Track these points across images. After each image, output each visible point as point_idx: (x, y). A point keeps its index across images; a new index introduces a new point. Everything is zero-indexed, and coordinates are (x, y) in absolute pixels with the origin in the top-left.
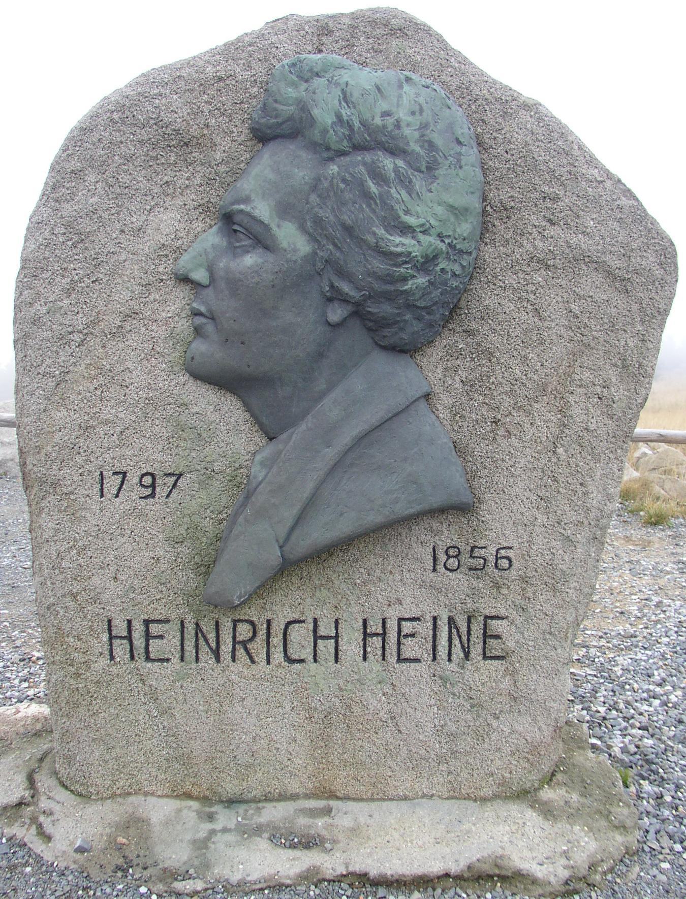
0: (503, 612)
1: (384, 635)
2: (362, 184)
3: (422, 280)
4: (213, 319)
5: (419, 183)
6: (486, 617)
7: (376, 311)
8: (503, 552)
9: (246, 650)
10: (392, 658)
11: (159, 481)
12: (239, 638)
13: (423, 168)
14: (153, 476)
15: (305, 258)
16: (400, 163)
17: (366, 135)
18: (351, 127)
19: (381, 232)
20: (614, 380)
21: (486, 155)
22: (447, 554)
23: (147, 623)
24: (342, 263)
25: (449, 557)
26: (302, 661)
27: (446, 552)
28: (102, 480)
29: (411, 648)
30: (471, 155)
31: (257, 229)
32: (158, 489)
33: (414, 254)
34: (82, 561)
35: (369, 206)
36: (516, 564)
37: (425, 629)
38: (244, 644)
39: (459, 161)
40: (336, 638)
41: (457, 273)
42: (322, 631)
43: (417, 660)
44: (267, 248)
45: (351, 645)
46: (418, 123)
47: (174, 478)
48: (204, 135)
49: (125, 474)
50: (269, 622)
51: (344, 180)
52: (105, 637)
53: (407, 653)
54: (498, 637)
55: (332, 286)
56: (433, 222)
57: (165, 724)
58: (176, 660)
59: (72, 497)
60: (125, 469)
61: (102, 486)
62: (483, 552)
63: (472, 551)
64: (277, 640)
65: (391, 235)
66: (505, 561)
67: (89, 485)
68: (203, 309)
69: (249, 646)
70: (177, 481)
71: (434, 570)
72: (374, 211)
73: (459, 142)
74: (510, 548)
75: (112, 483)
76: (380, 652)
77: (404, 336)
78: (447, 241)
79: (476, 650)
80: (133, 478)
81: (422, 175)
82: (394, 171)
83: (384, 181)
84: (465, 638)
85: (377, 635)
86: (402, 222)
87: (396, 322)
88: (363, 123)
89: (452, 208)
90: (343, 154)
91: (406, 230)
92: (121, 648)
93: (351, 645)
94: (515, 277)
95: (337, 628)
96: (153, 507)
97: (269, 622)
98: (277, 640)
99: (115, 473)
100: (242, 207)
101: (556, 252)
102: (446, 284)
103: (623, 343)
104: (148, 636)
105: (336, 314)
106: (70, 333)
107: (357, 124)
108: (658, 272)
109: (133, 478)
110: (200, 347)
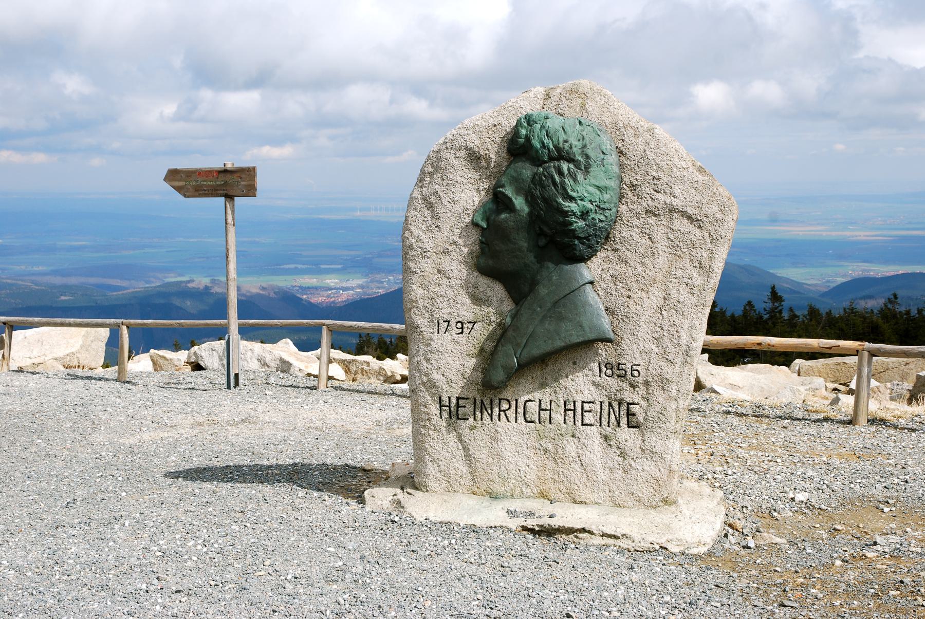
0: (636, 401)
1: (574, 410)
5: (580, 177)
6: (629, 404)
8: (635, 367)
10: (579, 424)
16: (571, 166)
18: (549, 149)
19: (560, 200)
20: (695, 274)
23: (458, 399)
29: (589, 418)
30: (613, 158)
38: (504, 411)
42: (543, 406)
43: (591, 425)
45: (558, 417)
52: (438, 406)
53: (586, 421)
54: (634, 415)
55: (540, 228)
64: (521, 410)
73: (603, 153)
79: (624, 421)
80: (453, 324)
88: (555, 146)
91: (572, 199)
93: (558, 417)
96: (462, 339)
97: (517, 401)
98: (521, 410)
104: (458, 406)
107: (551, 146)
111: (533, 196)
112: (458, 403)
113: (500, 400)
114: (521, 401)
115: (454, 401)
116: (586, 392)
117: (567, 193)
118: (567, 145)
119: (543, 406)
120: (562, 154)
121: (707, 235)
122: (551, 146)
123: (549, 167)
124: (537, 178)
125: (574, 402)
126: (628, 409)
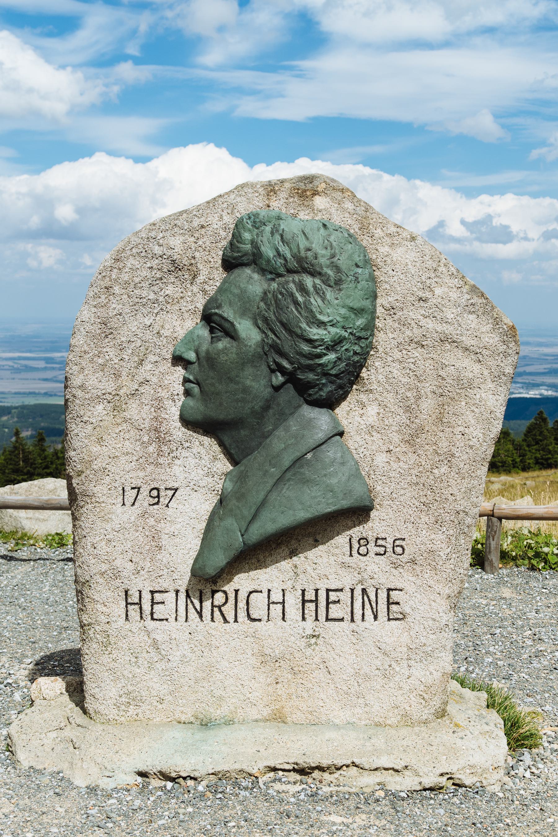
1: (316, 601)
2: (292, 295)
3: (332, 356)
4: (198, 384)
6: (389, 590)
7: (303, 377)
8: (398, 543)
11: (162, 493)
12: (216, 603)
13: (332, 284)
14: (158, 489)
15: (257, 345)
16: (317, 281)
17: (295, 264)
18: (285, 259)
20: (473, 421)
21: (379, 272)
22: (359, 543)
23: (152, 592)
24: (280, 346)
25: (360, 546)
26: (260, 620)
28: (124, 493)
31: (227, 325)
32: (161, 500)
33: (326, 340)
34: (108, 550)
35: (297, 309)
37: (345, 597)
38: (219, 607)
39: (357, 278)
41: (357, 352)
44: (232, 337)
46: (329, 254)
47: (173, 491)
48: (192, 264)
49: (139, 488)
50: (237, 591)
51: (281, 293)
54: (398, 603)
55: (274, 361)
56: (338, 319)
57: (164, 667)
58: (172, 619)
59: (103, 505)
60: (139, 485)
61: (124, 496)
63: (385, 552)
64: (242, 604)
65: (311, 328)
66: (398, 548)
67: (115, 496)
68: (191, 378)
70: (175, 493)
71: (351, 555)
72: (300, 314)
74: (404, 539)
75: (131, 494)
76: (314, 615)
77: (322, 393)
78: (349, 331)
80: (145, 491)
81: (331, 289)
82: (313, 287)
83: (306, 293)
84: (374, 605)
85: (311, 601)
86: (317, 320)
87: (318, 385)
89: (352, 309)
90: (280, 275)
91: (321, 324)
92: (134, 611)
93: (293, 610)
94: (400, 353)
95: (284, 595)
97: (237, 591)
98: (242, 604)
99: (133, 488)
100: (217, 311)
101: (427, 336)
102: (349, 360)
103: (478, 396)
104: (153, 603)
105: (279, 379)
106: (104, 394)
107: (289, 256)
109: (145, 491)
110: (191, 402)
111: (266, 320)
112: (153, 599)
113: (214, 592)
114: (242, 596)
115: (147, 597)
117: (314, 317)
118: (309, 254)
119: (273, 599)
120: (304, 266)
123: (287, 282)
124: (270, 296)
125: (317, 591)
126: (388, 595)
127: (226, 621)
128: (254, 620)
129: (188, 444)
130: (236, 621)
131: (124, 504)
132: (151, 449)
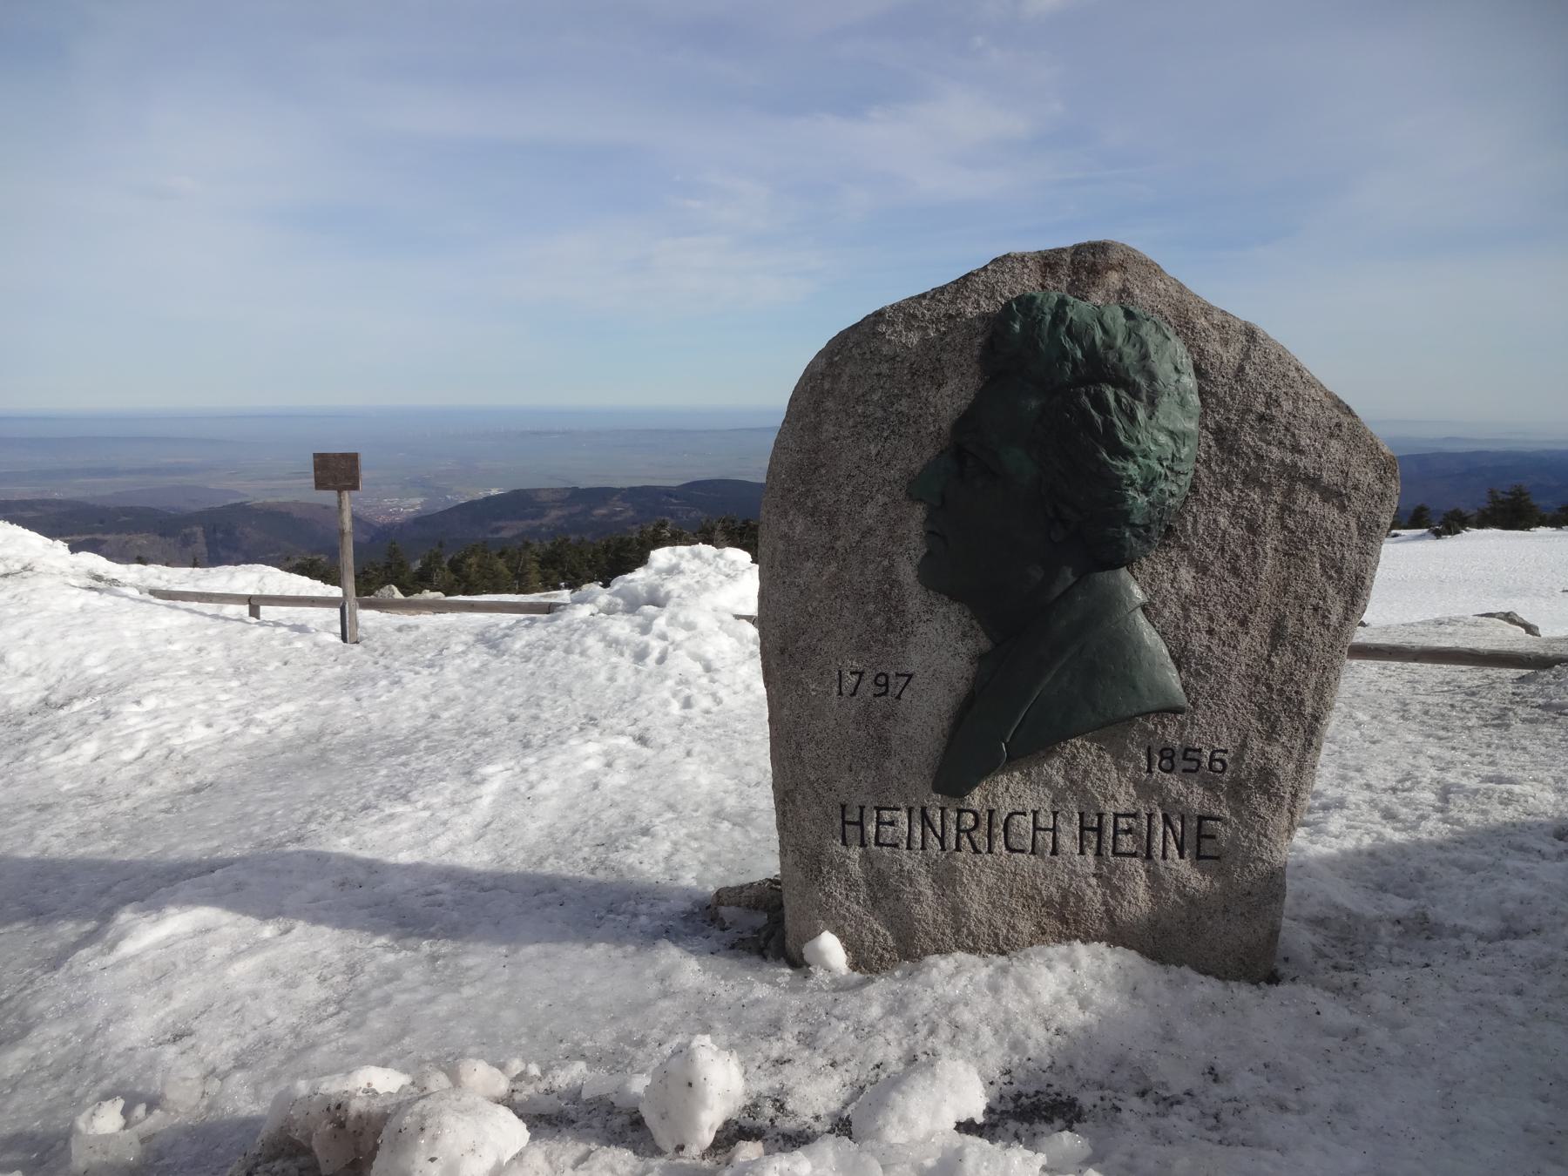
0: (1216, 812)
1: (1099, 831)
6: (1201, 819)
9: (969, 837)
11: (892, 681)
16: (1123, 393)
20: (1330, 591)
26: (1022, 851)
27: (1161, 753)
36: (1230, 766)
38: (968, 832)
40: (1054, 829)
49: (861, 674)
50: (991, 812)
52: (838, 823)
53: (1124, 848)
54: (1213, 837)
62: (1196, 755)
64: (999, 831)
69: (973, 834)
71: (1149, 771)
85: (1092, 829)
92: (852, 831)
97: (991, 812)
98: (999, 831)
104: (879, 823)
108: (1378, 487)
113: (960, 812)
116: (1122, 798)
121: (1353, 525)
122: (1079, 354)
123: (1078, 395)
125: (1100, 816)
126: (1200, 826)
127: (977, 851)
128: (1012, 850)
129: (928, 616)
130: (990, 851)
131: (840, 693)
132: (878, 620)
